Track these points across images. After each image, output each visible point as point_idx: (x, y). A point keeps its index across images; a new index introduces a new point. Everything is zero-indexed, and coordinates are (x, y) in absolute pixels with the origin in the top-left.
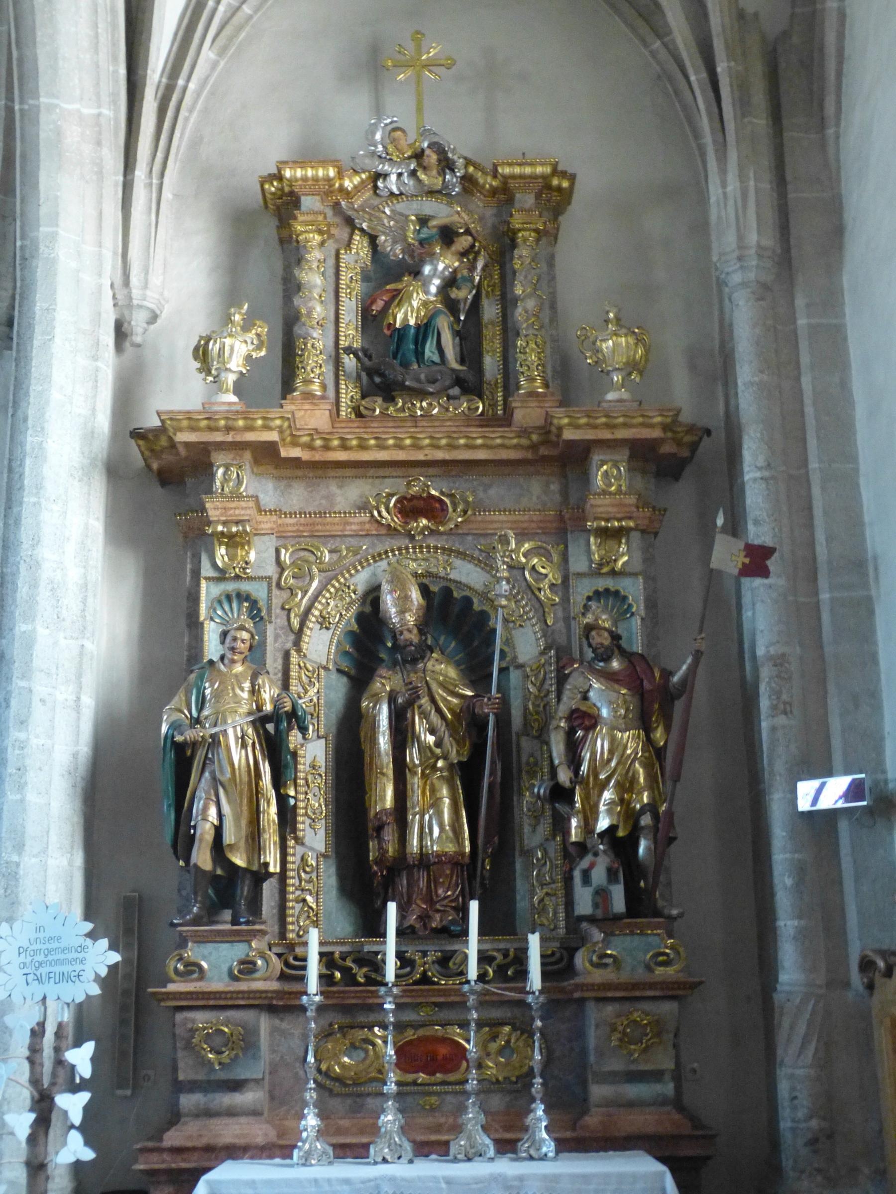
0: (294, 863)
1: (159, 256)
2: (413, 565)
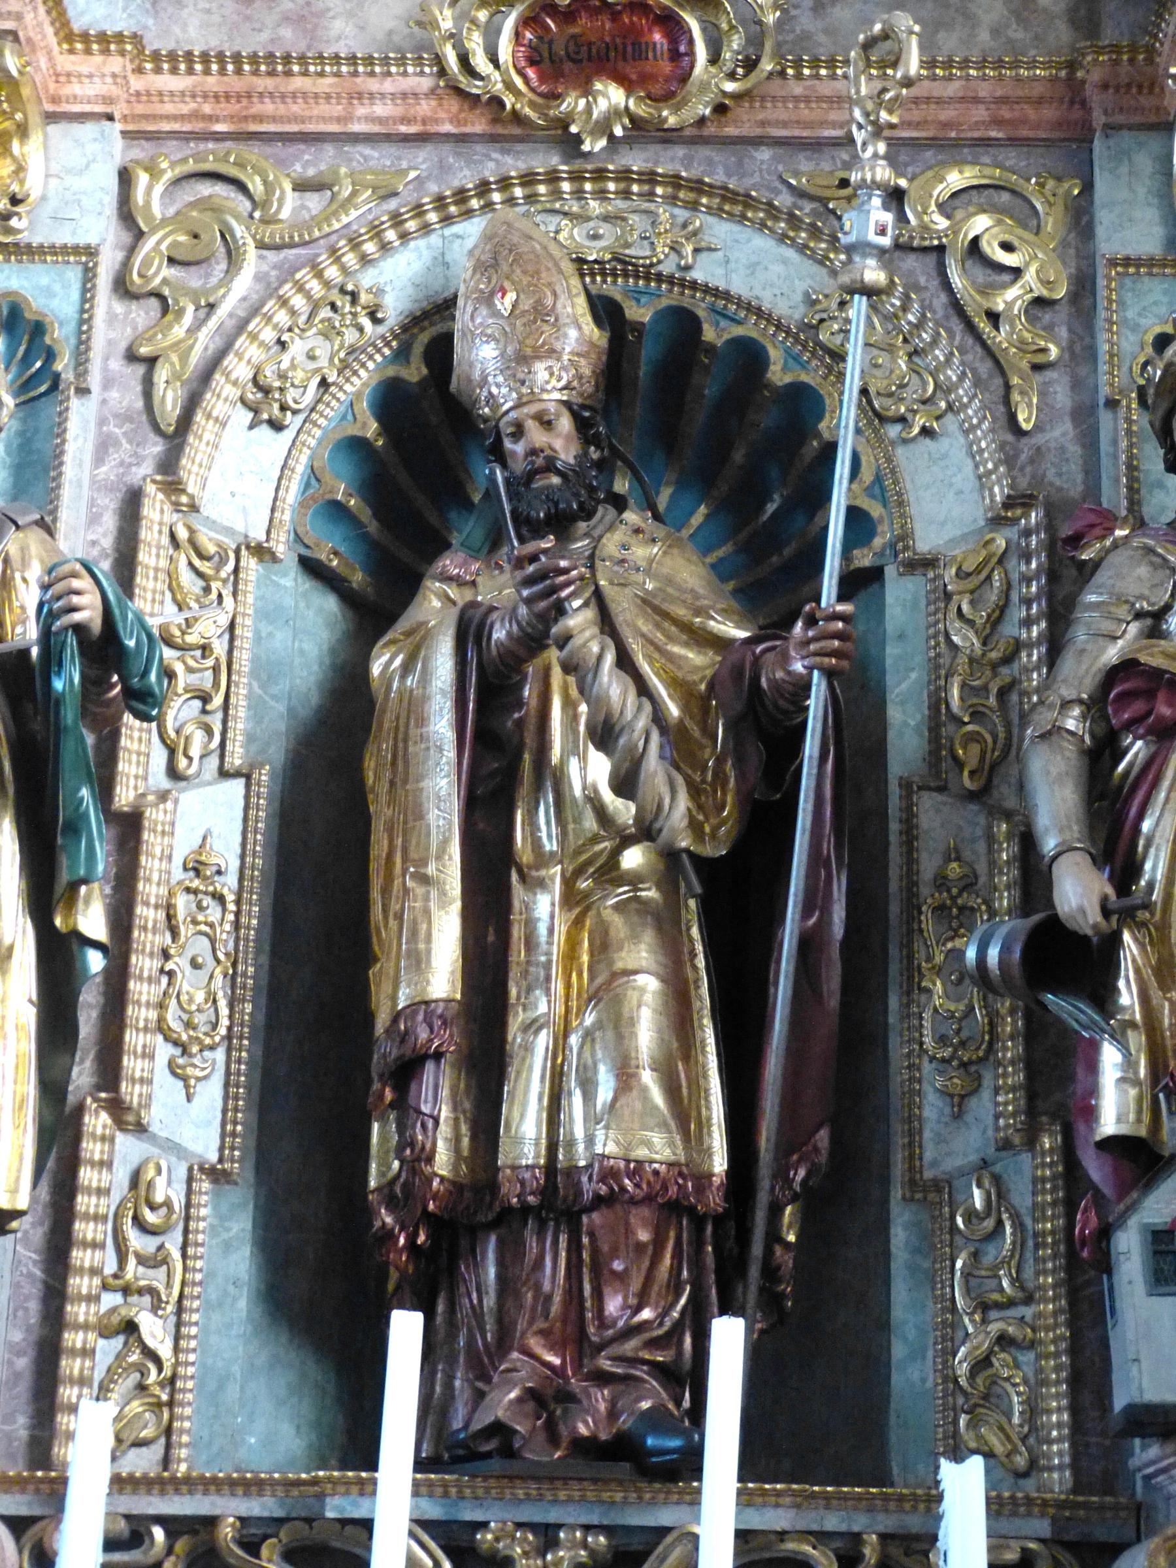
0: (102, 1192)
2: (572, 235)
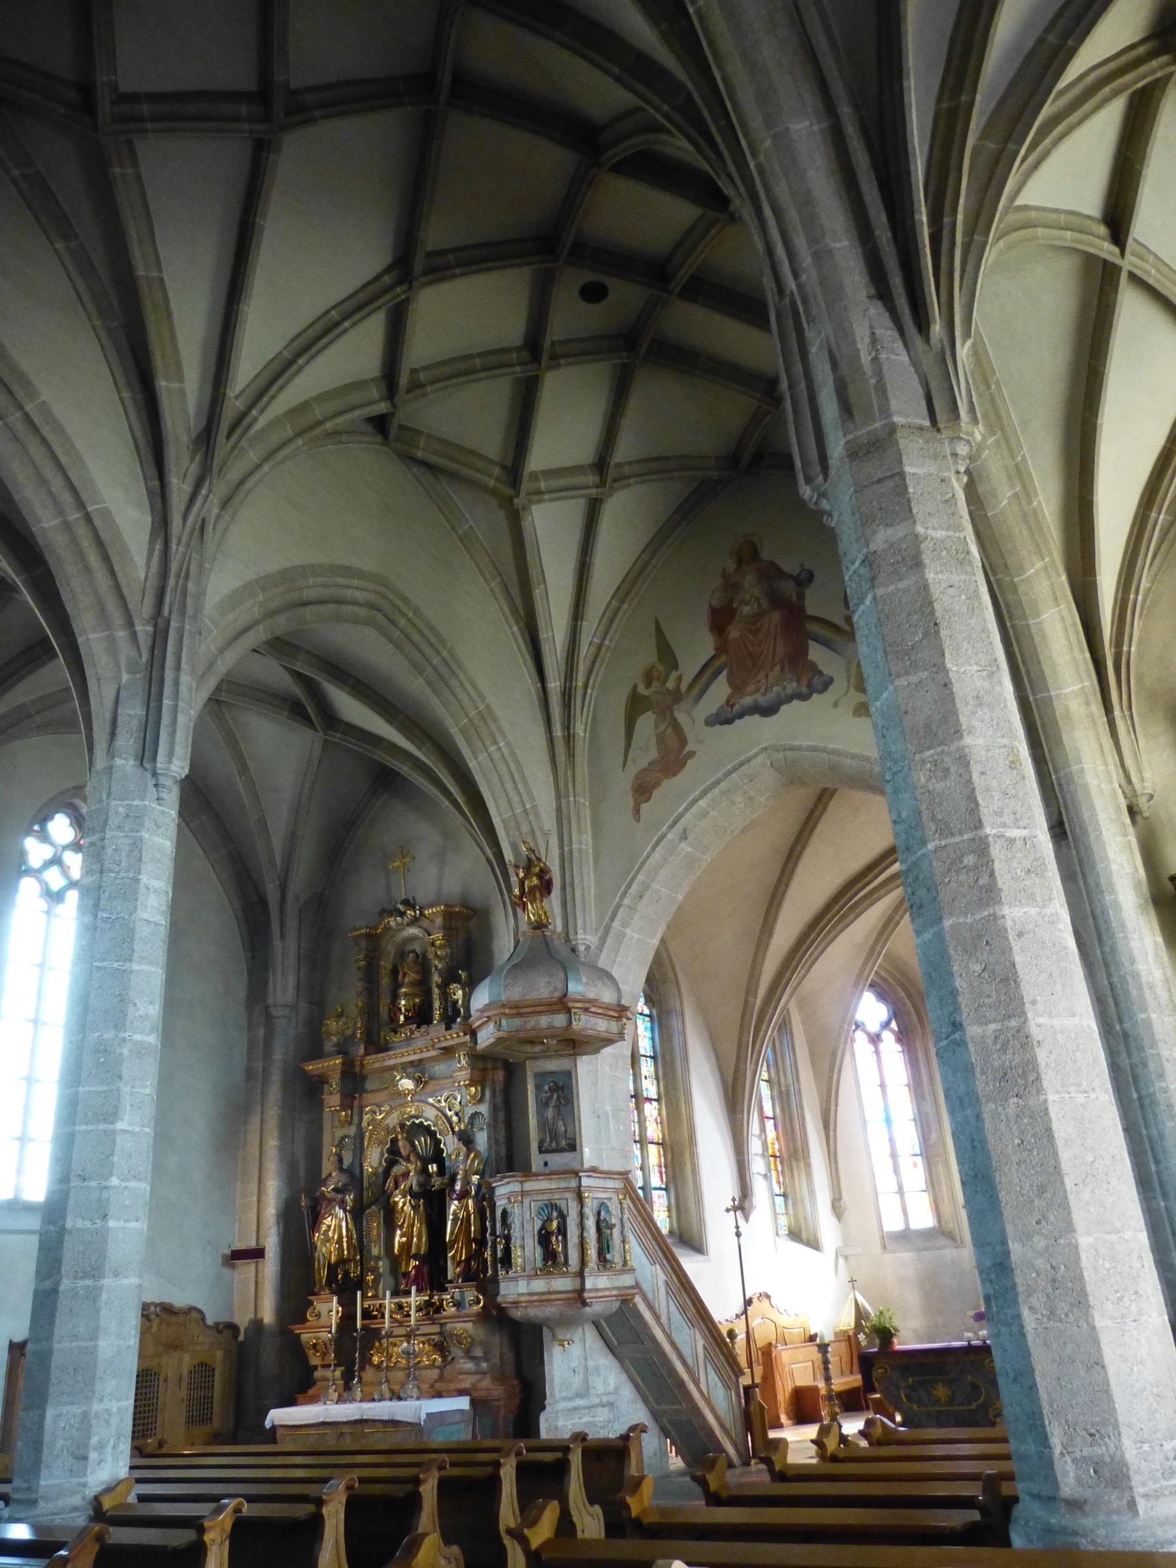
1: (1144, 758)
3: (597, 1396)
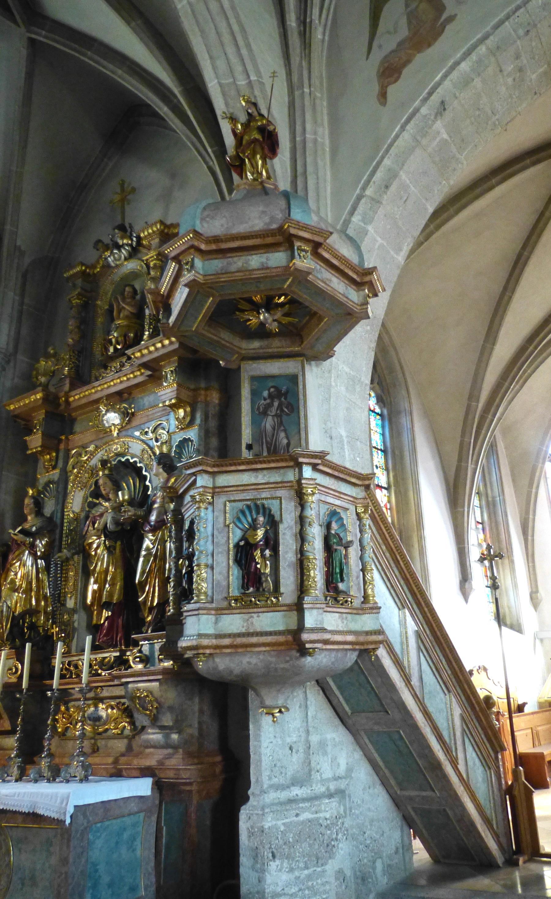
3: (323, 781)
